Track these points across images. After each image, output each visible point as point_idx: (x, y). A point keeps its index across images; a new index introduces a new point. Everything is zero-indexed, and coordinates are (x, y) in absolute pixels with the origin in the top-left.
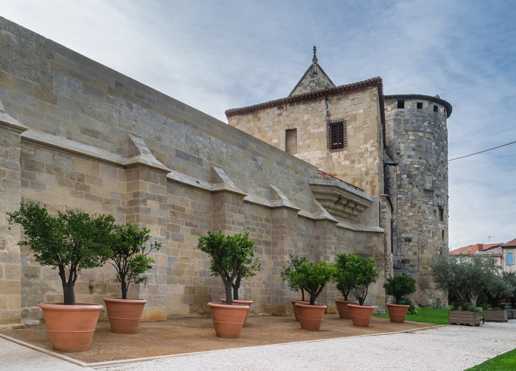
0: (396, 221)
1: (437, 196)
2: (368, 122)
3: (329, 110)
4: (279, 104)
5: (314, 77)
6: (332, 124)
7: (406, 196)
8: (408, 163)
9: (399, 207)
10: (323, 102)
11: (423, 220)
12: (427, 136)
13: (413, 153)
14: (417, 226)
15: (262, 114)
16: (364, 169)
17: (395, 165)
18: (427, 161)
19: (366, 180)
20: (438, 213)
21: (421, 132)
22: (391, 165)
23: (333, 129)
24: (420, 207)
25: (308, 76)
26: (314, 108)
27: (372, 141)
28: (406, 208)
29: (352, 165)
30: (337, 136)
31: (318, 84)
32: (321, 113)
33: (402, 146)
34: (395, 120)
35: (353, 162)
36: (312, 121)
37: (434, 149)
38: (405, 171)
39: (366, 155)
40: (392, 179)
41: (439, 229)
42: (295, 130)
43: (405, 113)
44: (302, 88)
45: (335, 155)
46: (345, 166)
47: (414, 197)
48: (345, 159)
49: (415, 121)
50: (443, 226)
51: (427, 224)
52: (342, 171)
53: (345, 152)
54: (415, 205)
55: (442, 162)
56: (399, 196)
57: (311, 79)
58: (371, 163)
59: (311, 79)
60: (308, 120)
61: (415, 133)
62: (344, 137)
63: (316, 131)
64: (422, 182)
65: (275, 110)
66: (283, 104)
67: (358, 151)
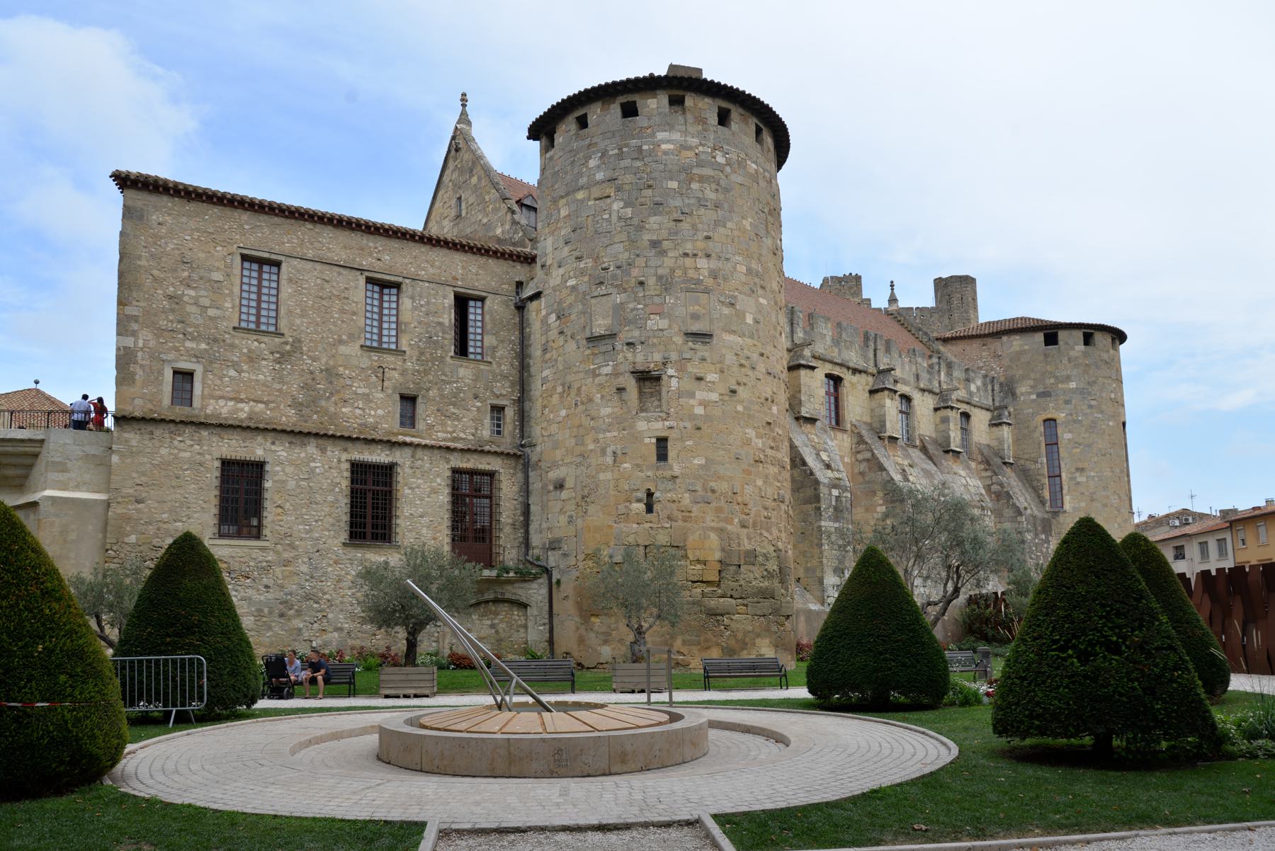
11: (586, 422)
14: (573, 440)
18: (596, 259)
24: (579, 389)
37: (620, 218)
41: (637, 438)
56: (546, 373)
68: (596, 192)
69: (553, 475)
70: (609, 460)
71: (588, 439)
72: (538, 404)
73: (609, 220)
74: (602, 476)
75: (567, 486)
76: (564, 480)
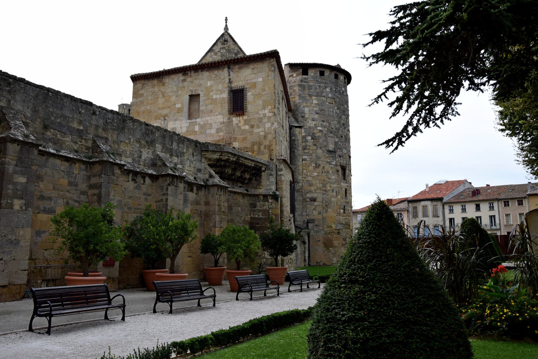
0: (302, 181)
1: (340, 156)
2: (267, 89)
3: (231, 77)
4: (184, 71)
5: (225, 45)
6: (234, 90)
7: (311, 157)
8: (313, 125)
9: (304, 168)
10: (226, 70)
11: (327, 180)
12: (329, 100)
13: (316, 116)
14: (321, 185)
15: (167, 80)
16: (262, 133)
17: (300, 127)
18: (329, 124)
19: (264, 144)
20: (340, 172)
21: (324, 97)
22: (296, 127)
23: (234, 95)
24: (324, 167)
25: (219, 44)
26: (217, 75)
27: (270, 107)
28: (311, 168)
29: (251, 130)
30: (237, 102)
31: (229, 51)
32: (224, 80)
33: (306, 110)
34: (300, 85)
35: (252, 127)
36: (215, 88)
38: (309, 133)
39: (264, 121)
40: (298, 140)
42: (199, 95)
43: (309, 80)
44: (212, 54)
45: (235, 120)
46: (244, 130)
47: (318, 158)
48: (245, 124)
49: (318, 87)
50: (345, 185)
51: (331, 183)
52: (242, 135)
53: (245, 117)
54: (319, 165)
55: (344, 124)
56: (304, 157)
57: (222, 46)
58: (268, 128)
59: (222, 46)
60: (211, 86)
61: (318, 98)
62: (245, 103)
63: (218, 96)
64: (325, 143)
65: (181, 77)
66: (188, 71)
67: (257, 116)
68: (329, 100)
69: (308, 195)
70: (335, 194)
71: (328, 186)
72: (301, 168)
73: (333, 112)
74: (333, 199)
75: (317, 200)
76: (316, 198)
